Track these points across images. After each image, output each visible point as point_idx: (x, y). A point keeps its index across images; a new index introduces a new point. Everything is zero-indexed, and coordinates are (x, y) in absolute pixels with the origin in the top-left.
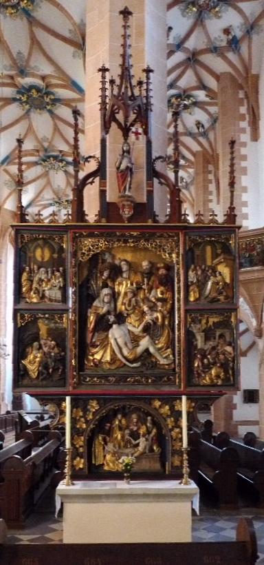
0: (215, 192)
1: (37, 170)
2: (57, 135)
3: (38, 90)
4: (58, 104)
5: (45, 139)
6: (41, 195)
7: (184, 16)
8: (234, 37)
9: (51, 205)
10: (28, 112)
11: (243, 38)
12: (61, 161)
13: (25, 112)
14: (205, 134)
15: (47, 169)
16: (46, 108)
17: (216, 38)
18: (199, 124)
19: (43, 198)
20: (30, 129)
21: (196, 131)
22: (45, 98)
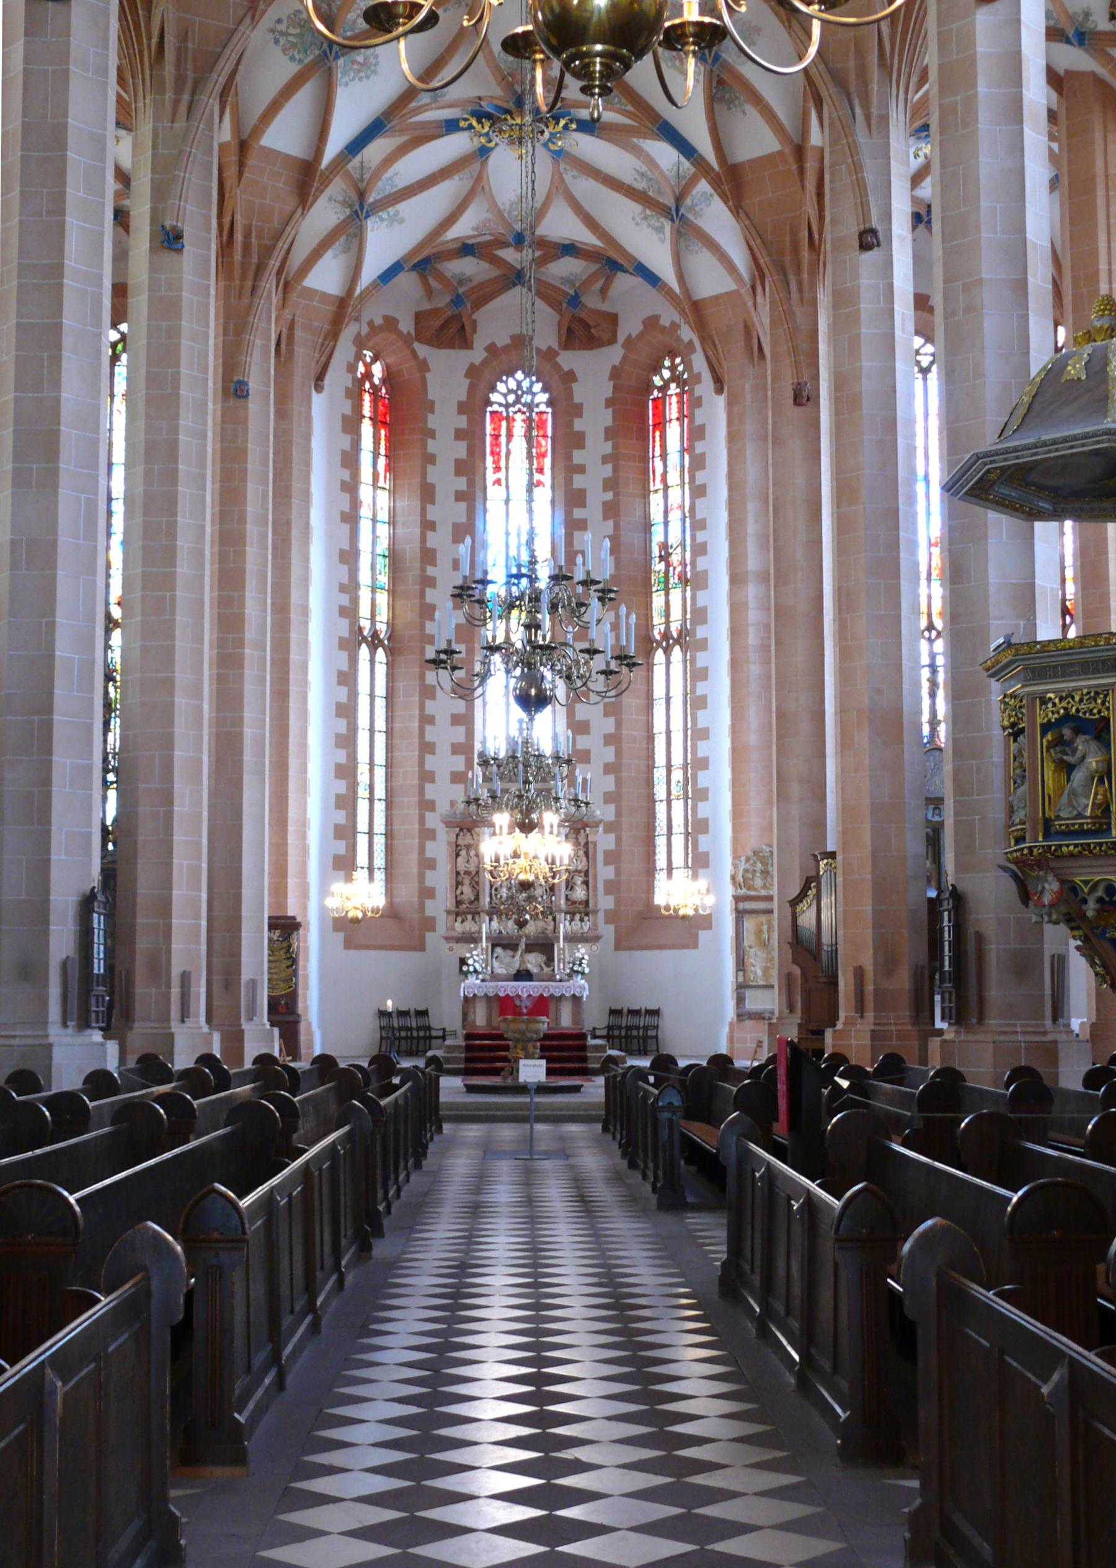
9: (451, 126)
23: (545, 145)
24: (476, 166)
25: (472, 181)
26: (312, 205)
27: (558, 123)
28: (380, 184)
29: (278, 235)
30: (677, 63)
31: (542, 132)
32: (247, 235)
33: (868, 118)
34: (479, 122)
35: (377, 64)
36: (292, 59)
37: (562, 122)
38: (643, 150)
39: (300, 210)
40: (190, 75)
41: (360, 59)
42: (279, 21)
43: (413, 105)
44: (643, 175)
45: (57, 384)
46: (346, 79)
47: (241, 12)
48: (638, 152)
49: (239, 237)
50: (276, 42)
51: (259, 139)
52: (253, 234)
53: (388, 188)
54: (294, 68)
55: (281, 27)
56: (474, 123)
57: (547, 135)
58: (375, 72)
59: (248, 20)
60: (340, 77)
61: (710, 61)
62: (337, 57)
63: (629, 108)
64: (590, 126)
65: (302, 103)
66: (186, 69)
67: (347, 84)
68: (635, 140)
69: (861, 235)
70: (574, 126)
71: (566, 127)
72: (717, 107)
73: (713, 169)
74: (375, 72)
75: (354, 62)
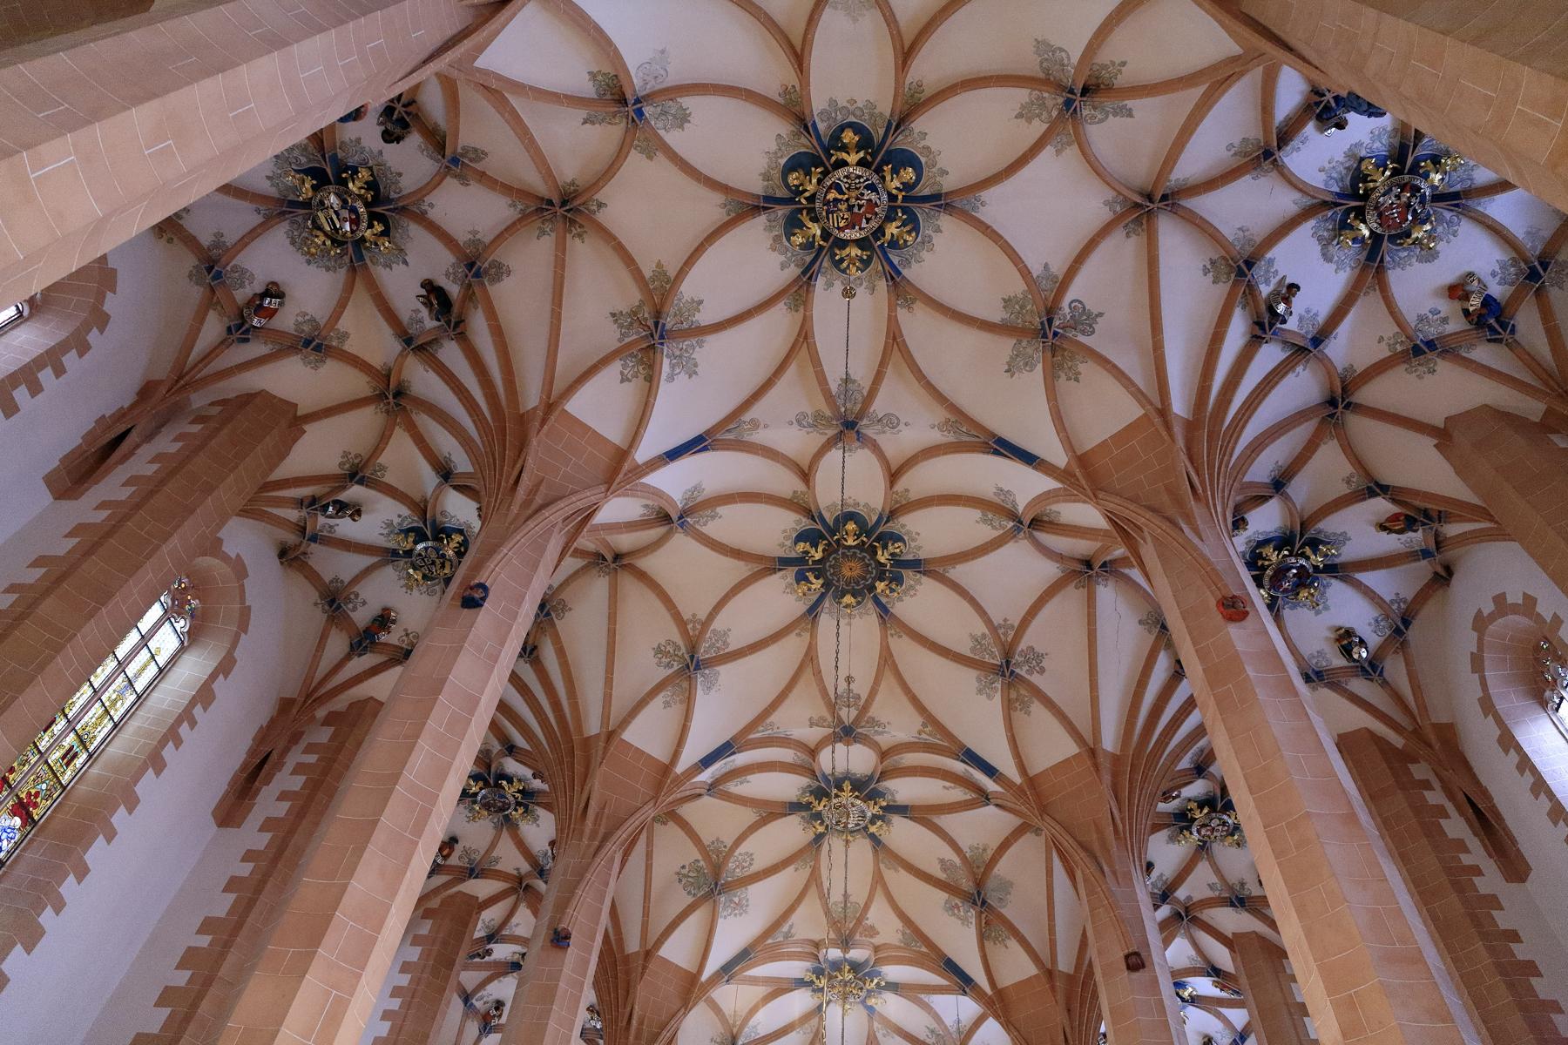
0: (1474, 843)
1: (790, 833)
2: (889, 683)
3: (864, 529)
4: (908, 574)
5: (850, 698)
6: (785, 928)
7: (1327, 258)
8: (1488, 302)
9: (800, 983)
10: (813, 612)
11: (1516, 298)
12: (873, 796)
13: (804, 608)
14: (1372, 669)
15: (821, 829)
16: (872, 588)
17: (1421, 319)
18: (1346, 639)
19: (787, 935)
20: (810, 657)
21: (1339, 661)
22: (880, 552)
23: (863, 1002)
24: (814, 1022)
25: (812, 1035)
26: (691, 1009)
27: (872, 981)
28: (746, 1029)
29: (663, 1026)
30: (956, 911)
31: (861, 989)
32: (641, 1023)
33: (1114, 873)
34: (818, 978)
35: (747, 906)
36: (689, 893)
37: (876, 981)
38: (932, 1008)
39: (683, 1010)
40: (602, 830)
41: (736, 900)
42: (683, 867)
43: (770, 941)
44: (932, 1031)
45: (351, 871)
46: (725, 913)
47: (648, 798)
48: (927, 1007)
49: (634, 1022)
50: (680, 881)
51: (658, 950)
52: (645, 1023)
53: (753, 1035)
54: (690, 899)
55: (684, 871)
56: (815, 979)
57: (863, 994)
58: (746, 912)
59: (651, 804)
60: (722, 912)
61: (979, 903)
62: (720, 894)
63: (924, 949)
64: (894, 987)
65: (691, 928)
66: (600, 826)
67: (725, 917)
68: (923, 996)
69: (1127, 957)
70: (883, 984)
71: (878, 984)
72: (986, 943)
73: (986, 994)
74: (746, 912)
75: (731, 901)
